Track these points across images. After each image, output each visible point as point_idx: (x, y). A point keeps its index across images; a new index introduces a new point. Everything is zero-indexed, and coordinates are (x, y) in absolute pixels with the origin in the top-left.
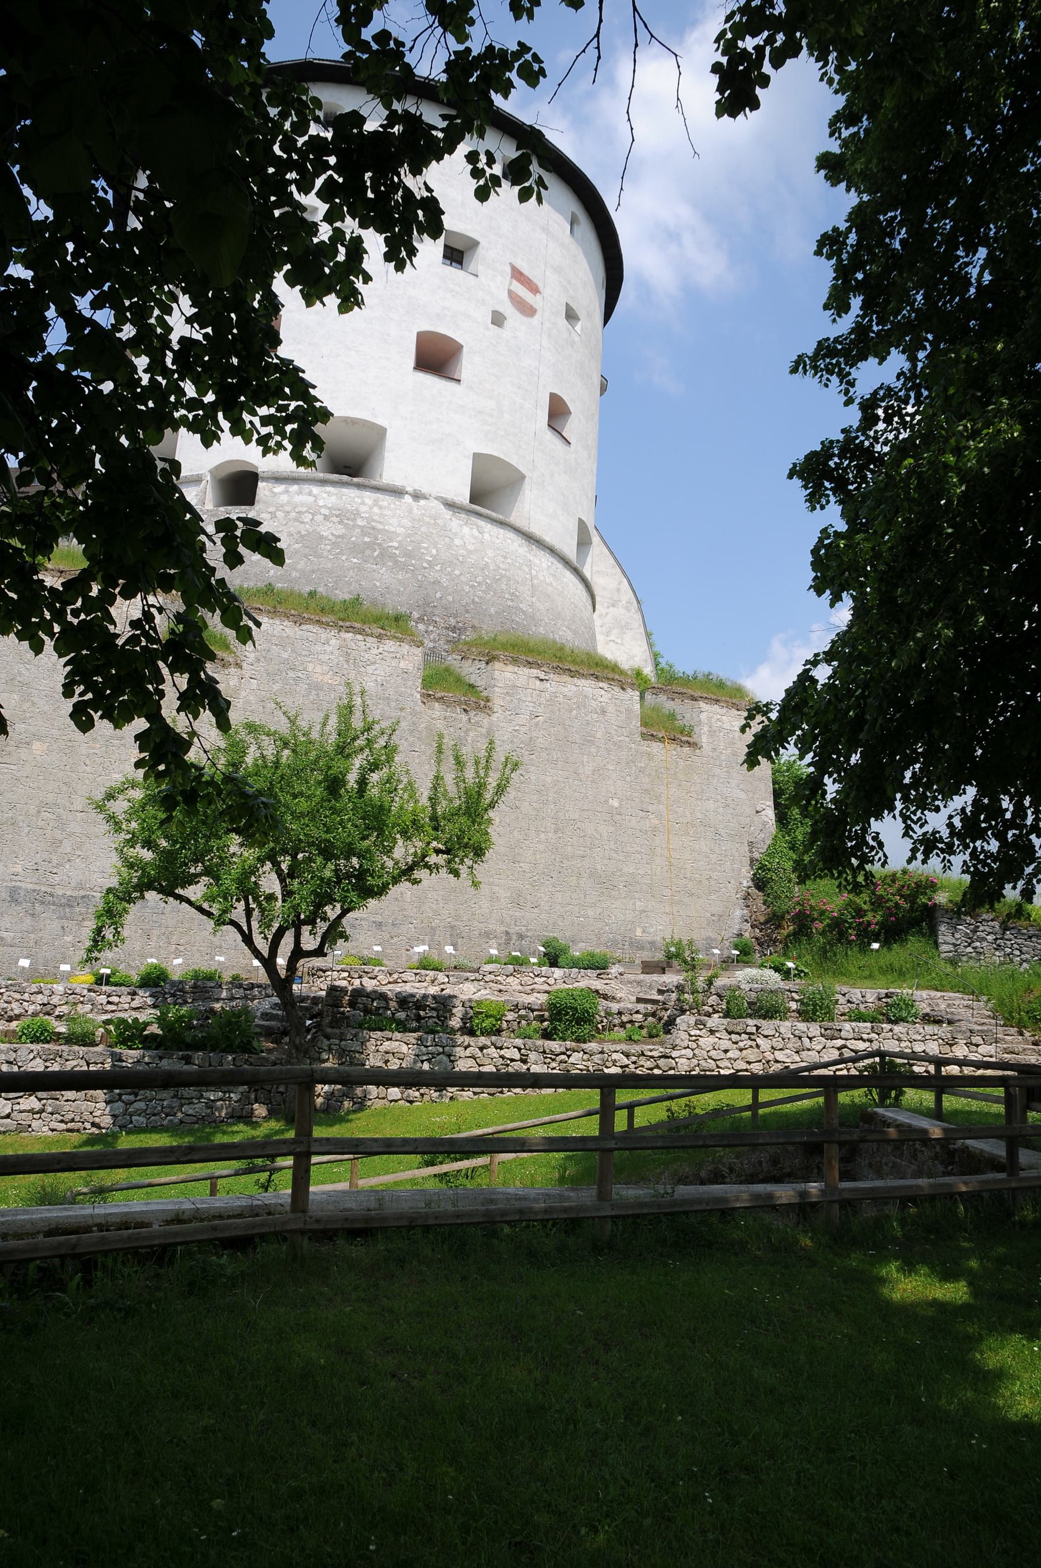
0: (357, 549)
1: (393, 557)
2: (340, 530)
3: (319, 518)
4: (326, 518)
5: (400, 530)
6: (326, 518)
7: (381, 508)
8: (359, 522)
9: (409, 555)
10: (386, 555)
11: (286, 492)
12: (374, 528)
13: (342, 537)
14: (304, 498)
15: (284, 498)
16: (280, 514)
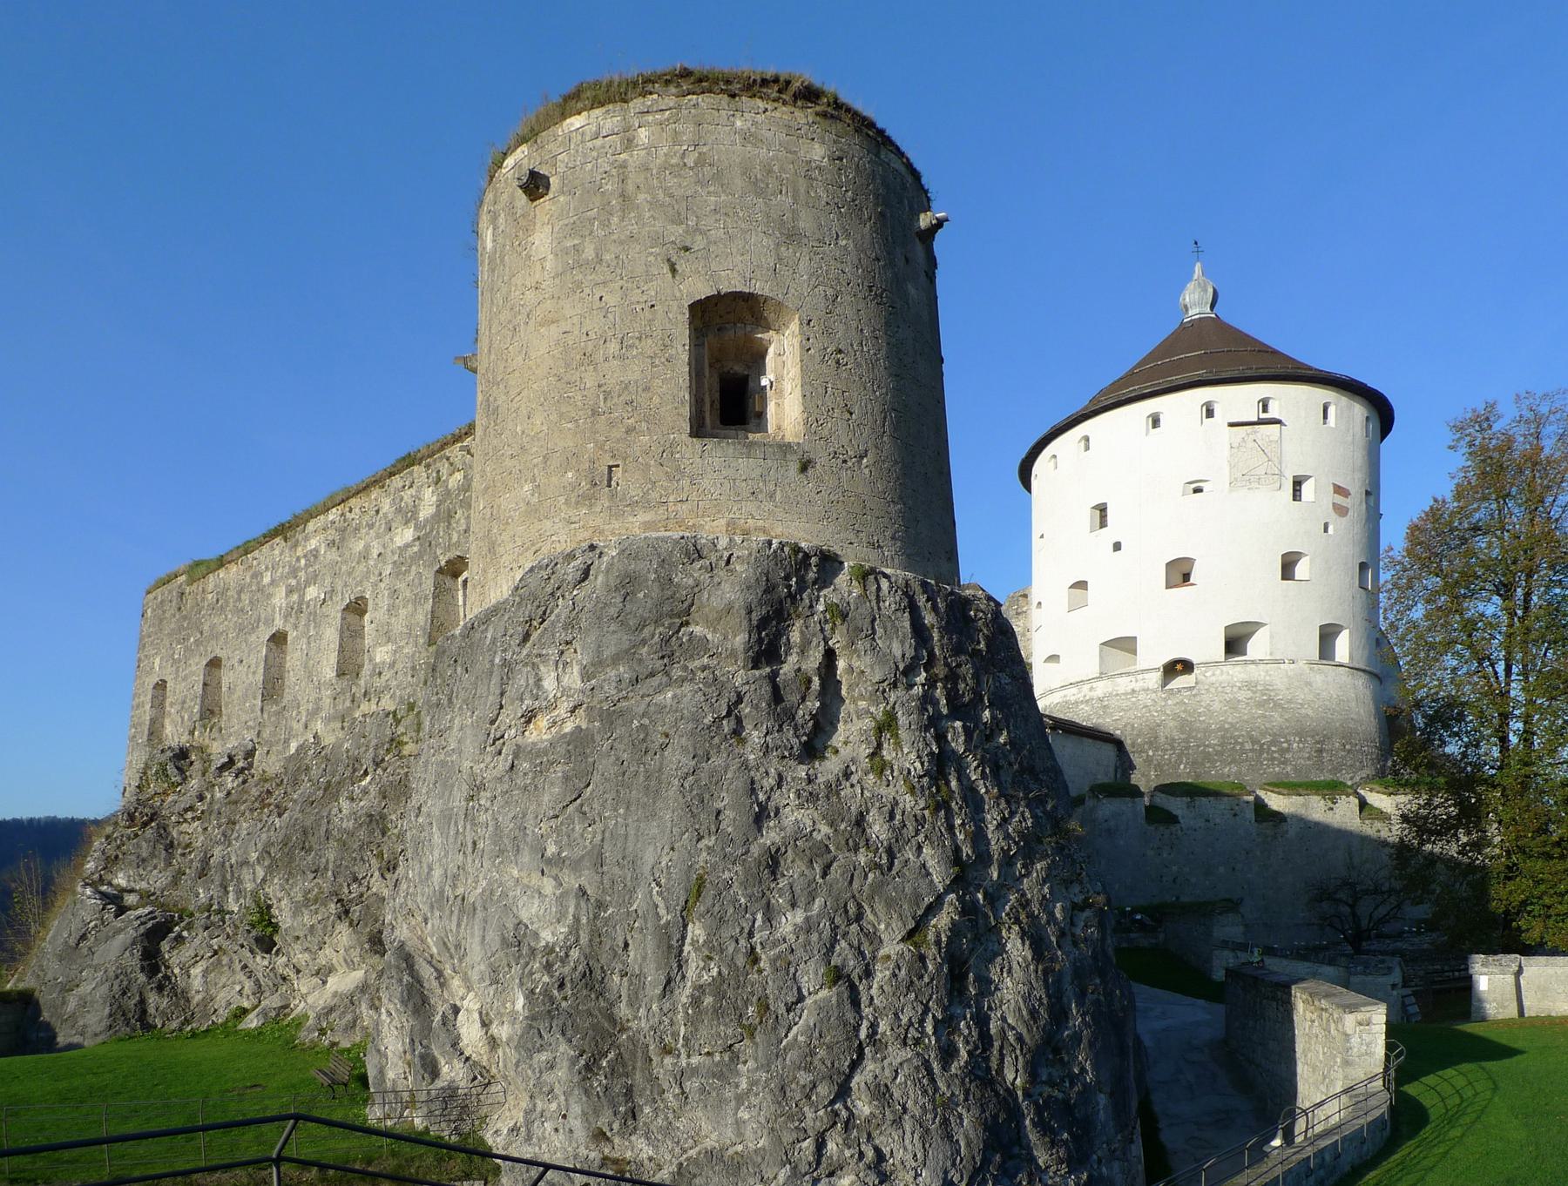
0: (1260, 705)
1: (1280, 706)
2: (1250, 694)
3: (1235, 689)
4: (1240, 688)
5: (1283, 687)
6: (1240, 688)
7: (1270, 675)
8: (1259, 688)
9: (1290, 702)
10: (1277, 705)
11: (1214, 675)
12: (1268, 690)
13: (1251, 698)
14: (1224, 677)
15: (1213, 679)
16: (1212, 690)
